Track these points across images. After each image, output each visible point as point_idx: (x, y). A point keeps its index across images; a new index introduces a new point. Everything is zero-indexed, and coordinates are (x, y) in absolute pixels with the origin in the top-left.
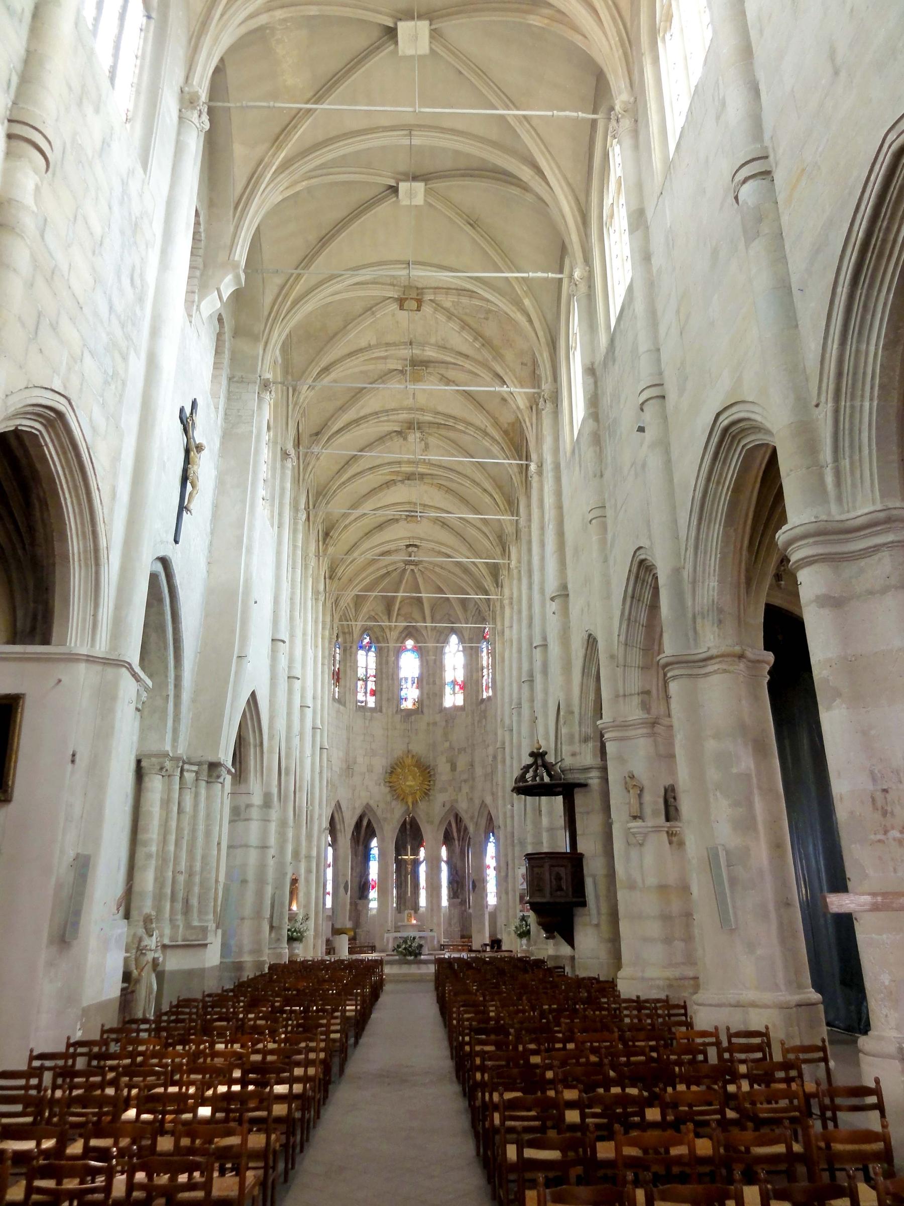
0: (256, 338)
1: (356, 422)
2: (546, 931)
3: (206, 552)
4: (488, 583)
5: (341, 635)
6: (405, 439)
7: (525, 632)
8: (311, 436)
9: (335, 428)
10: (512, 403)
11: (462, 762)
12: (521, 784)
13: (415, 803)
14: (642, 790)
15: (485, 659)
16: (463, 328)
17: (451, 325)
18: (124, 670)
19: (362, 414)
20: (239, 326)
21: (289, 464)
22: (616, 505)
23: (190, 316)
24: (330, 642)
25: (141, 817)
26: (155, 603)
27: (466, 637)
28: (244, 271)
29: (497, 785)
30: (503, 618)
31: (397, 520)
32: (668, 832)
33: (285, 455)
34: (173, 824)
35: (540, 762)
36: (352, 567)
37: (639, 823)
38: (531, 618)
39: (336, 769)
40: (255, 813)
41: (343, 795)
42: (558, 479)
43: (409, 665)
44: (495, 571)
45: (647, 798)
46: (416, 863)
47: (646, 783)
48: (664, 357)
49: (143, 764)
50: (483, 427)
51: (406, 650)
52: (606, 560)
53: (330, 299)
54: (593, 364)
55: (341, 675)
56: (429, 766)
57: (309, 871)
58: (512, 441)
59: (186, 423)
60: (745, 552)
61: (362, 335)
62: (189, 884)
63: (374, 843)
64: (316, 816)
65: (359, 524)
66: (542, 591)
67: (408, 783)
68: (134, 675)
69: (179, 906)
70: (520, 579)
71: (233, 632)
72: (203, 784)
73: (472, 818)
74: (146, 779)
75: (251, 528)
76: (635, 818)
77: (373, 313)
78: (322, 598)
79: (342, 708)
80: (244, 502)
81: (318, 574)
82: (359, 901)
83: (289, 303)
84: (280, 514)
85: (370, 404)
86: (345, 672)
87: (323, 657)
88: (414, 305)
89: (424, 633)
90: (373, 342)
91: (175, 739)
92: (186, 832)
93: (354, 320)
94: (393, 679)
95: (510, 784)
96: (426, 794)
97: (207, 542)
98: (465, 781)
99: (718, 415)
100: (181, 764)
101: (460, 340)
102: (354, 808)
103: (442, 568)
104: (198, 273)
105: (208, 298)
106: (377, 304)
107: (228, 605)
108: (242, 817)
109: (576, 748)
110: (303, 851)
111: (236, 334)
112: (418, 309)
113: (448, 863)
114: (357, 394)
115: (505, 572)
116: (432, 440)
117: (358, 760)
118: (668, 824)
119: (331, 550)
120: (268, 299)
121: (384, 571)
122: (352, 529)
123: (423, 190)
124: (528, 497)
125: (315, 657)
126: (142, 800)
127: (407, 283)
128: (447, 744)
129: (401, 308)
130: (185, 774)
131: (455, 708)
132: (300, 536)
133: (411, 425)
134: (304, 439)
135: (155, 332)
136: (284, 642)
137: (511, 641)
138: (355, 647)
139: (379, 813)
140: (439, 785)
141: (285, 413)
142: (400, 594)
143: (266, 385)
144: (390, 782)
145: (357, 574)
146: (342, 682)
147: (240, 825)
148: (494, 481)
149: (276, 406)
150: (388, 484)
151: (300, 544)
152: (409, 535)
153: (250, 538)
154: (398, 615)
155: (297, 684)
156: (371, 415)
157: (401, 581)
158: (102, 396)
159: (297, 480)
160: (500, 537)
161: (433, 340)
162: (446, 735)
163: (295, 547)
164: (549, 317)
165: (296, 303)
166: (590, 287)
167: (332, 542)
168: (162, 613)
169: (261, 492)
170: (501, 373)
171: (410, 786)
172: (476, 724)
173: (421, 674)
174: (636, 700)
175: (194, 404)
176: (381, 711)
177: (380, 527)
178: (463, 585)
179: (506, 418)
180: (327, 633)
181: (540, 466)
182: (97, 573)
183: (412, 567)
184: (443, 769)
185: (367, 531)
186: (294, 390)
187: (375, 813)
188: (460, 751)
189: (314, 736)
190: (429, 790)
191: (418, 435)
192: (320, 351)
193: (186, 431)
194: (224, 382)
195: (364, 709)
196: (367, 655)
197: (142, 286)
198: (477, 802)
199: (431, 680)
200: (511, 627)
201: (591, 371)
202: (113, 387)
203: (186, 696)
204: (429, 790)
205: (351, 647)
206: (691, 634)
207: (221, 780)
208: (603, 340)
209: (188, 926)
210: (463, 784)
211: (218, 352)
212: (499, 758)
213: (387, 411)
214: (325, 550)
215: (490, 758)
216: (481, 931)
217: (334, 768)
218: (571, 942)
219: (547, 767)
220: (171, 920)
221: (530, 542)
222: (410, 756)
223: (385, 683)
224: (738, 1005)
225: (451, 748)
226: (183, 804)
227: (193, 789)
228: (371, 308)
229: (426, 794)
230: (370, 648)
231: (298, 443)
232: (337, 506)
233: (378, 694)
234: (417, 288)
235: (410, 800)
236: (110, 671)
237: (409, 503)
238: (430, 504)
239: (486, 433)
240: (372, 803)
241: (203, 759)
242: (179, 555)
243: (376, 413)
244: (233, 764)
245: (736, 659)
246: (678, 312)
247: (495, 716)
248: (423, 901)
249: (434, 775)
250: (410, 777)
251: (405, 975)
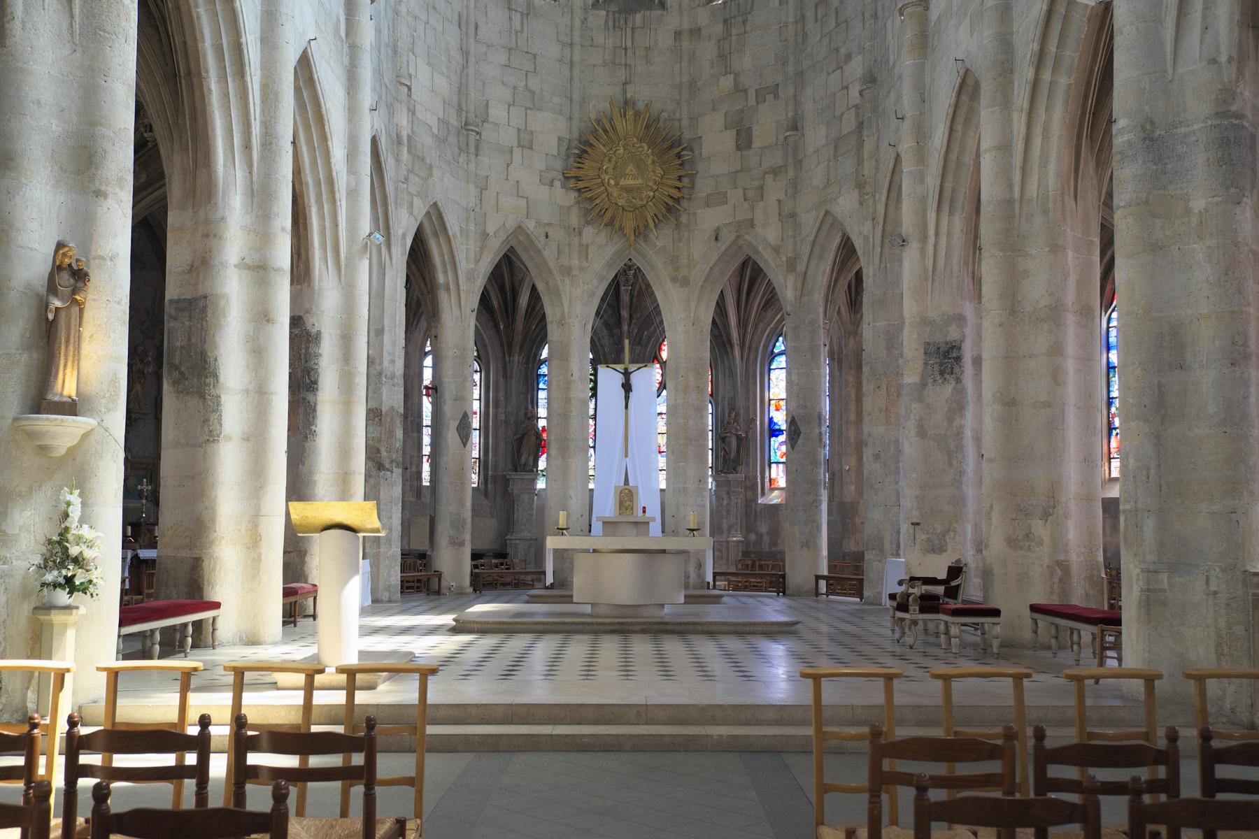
11: (767, 124)
13: (641, 232)
56: (679, 142)
67: (623, 182)
73: (791, 265)
82: (514, 476)
96: (669, 209)
98: (775, 171)
102: (485, 235)
117: (492, 111)
128: (727, 83)
139: (549, 253)
140: (704, 187)
144: (578, 179)
171: (629, 190)
172: (810, 14)
184: (715, 141)
188: (760, 97)
190: (677, 200)
198: (809, 221)
204: (677, 200)
210: (769, 178)
216: (810, 543)
217: (418, 114)
222: (630, 113)
225: (739, 90)
229: (672, 208)
235: (629, 224)
240: (530, 225)
250: (631, 168)
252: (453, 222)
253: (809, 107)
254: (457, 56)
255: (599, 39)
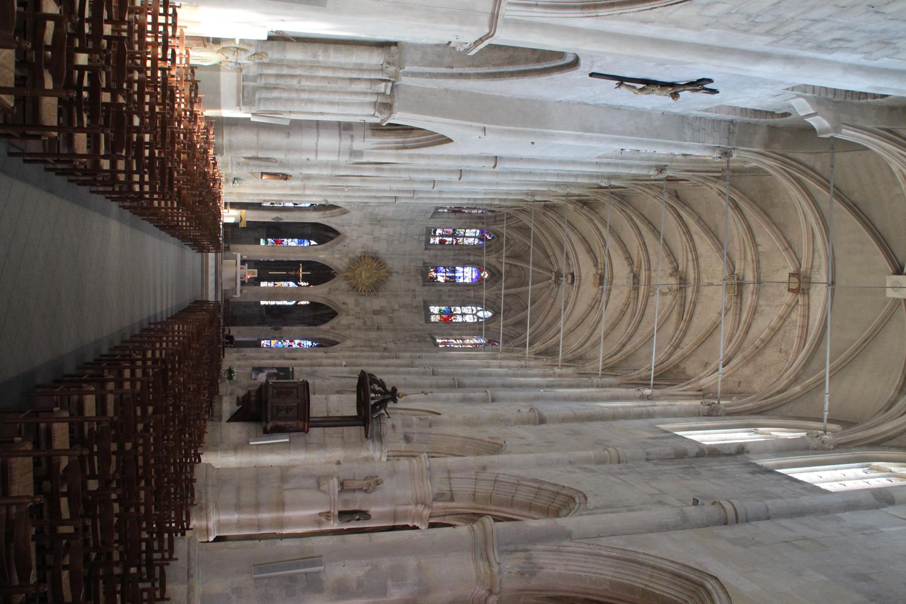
0: (767, 146)
1: (688, 232)
2: (243, 397)
3: (579, 100)
4: (538, 346)
5: (493, 214)
6: (671, 275)
7: (499, 381)
8: (676, 191)
9: (682, 213)
10: (705, 373)
11: (381, 320)
12: (368, 380)
13: (347, 278)
14: (366, 491)
15: (471, 341)
16: (772, 329)
17: (775, 318)
18: (487, 30)
19: (695, 237)
20: (781, 132)
21: (653, 172)
22: (622, 474)
23: (793, 89)
24: (487, 205)
25: (348, 47)
26: (536, 57)
27: (490, 325)
28: (832, 138)
29: (362, 351)
30: (507, 359)
31: (596, 265)
32: (329, 512)
33: (661, 169)
34: (341, 74)
35: (388, 396)
36: (553, 225)
37: (337, 489)
38: (511, 386)
39: (377, 210)
40: (346, 143)
41: (355, 216)
42: (639, 416)
43: (466, 275)
44: (550, 353)
45: (359, 496)
46: (296, 280)
47: (372, 496)
48: (762, 525)
49: (393, 48)
50: (682, 345)
51: (480, 270)
52: (570, 463)
53: (800, 211)
54: (748, 452)
55: (458, 214)
56: (377, 291)
57: (293, 188)
58: (669, 371)
59: (699, 85)
60: (585, 596)
61: (767, 239)
62: (290, 89)
63: (313, 242)
64: (339, 193)
65: (594, 232)
66: (537, 398)
68: (481, 40)
69: (272, 81)
70: (544, 376)
71: (507, 124)
72: (374, 99)
73: (333, 328)
74: (380, 51)
75: (599, 139)
76: (342, 484)
77: (786, 249)
78: (529, 198)
79: (430, 215)
80: (623, 133)
81: (549, 196)
83: (798, 175)
84: (608, 164)
85: (704, 246)
86: (461, 218)
87: (475, 199)
88: (794, 286)
89: (494, 288)
90: (760, 249)
91: (413, 74)
92: (334, 85)
93: (781, 232)
94: (454, 259)
95: (369, 370)
96: (354, 288)
97: (588, 101)
98: (365, 323)
99: (715, 578)
100: (392, 79)
101: (761, 327)
103: (552, 304)
104: (830, 96)
105: (808, 105)
106: (795, 253)
107: (532, 118)
108: (343, 132)
109: (400, 430)
110: (309, 183)
111: (772, 128)
112: (789, 290)
113: (296, 305)
114: (712, 233)
115: (549, 363)
116: (669, 299)
118: (336, 513)
119: (571, 207)
120: (801, 157)
121: (550, 253)
122: (589, 226)
123: (900, 297)
124: (619, 386)
125: (477, 193)
126: (362, 48)
127: (813, 280)
128: (396, 307)
129: (791, 275)
130: (384, 84)
131: (429, 314)
132: (586, 181)
133: (683, 281)
134: (672, 186)
135: (788, 59)
136: (494, 167)
137: (489, 367)
138: (484, 226)
139: (339, 247)
140: (361, 299)
141: (698, 169)
142: (531, 268)
143: (726, 154)
145: (547, 228)
146: (452, 215)
147: (337, 132)
148: (632, 354)
149: (705, 161)
150: (629, 259)
151: (579, 180)
152: (583, 276)
153: (591, 138)
154: (511, 265)
155: (455, 177)
156: (694, 245)
157: (541, 268)
158: (737, 12)
159: (636, 179)
160: (581, 358)
161: (761, 302)
162: (404, 306)
163: (577, 176)
164: (784, 409)
165: (798, 180)
166: (815, 449)
167: (578, 208)
168: (527, 61)
169: (629, 148)
170: (732, 364)
171: (361, 274)
173: (459, 285)
174: (445, 488)
175: (714, 91)
176: (426, 249)
177: (590, 250)
178: (537, 324)
179: (691, 367)
180: (496, 202)
181: (648, 398)
182: (575, 7)
183: (553, 278)
184: (377, 303)
185: (587, 239)
186: (718, 178)
187: (338, 243)
188: (391, 318)
189: (407, 191)
191: (675, 287)
192: (753, 201)
193: (691, 84)
194: (730, 117)
195: (430, 233)
196: (475, 237)
197: (831, 49)
198: (347, 333)
199: (453, 293)
200: (501, 367)
201: (741, 450)
202: (744, 22)
203: (452, 84)
205: (483, 223)
206: (512, 547)
207: (377, 114)
208: (768, 462)
209: (256, 89)
210: (361, 321)
211: (756, 112)
212: (386, 354)
213: (697, 259)
214: (571, 202)
215: (384, 345)
218: (234, 418)
219: (383, 403)
220: (261, 75)
221: (578, 386)
223: (451, 253)
224: (189, 576)
225: (393, 311)
226: (357, 82)
227: (370, 91)
228: (791, 247)
229: (354, 288)
230: (480, 239)
231: (669, 179)
232: (612, 212)
233: (439, 247)
234: (808, 290)
235: (349, 274)
236: (486, 19)
237: (612, 277)
238: (611, 296)
239: (677, 347)
240: (348, 241)
241: (396, 99)
242: (579, 77)
243: (695, 250)
244: (390, 124)
245: (488, 588)
246: (805, 538)
247: (422, 351)
248: (263, 284)
249: (369, 296)
250: (368, 275)
251: (207, 271)
252: (345, 216)
253: (384, 333)
254: (401, 218)
255: (413, 264)
